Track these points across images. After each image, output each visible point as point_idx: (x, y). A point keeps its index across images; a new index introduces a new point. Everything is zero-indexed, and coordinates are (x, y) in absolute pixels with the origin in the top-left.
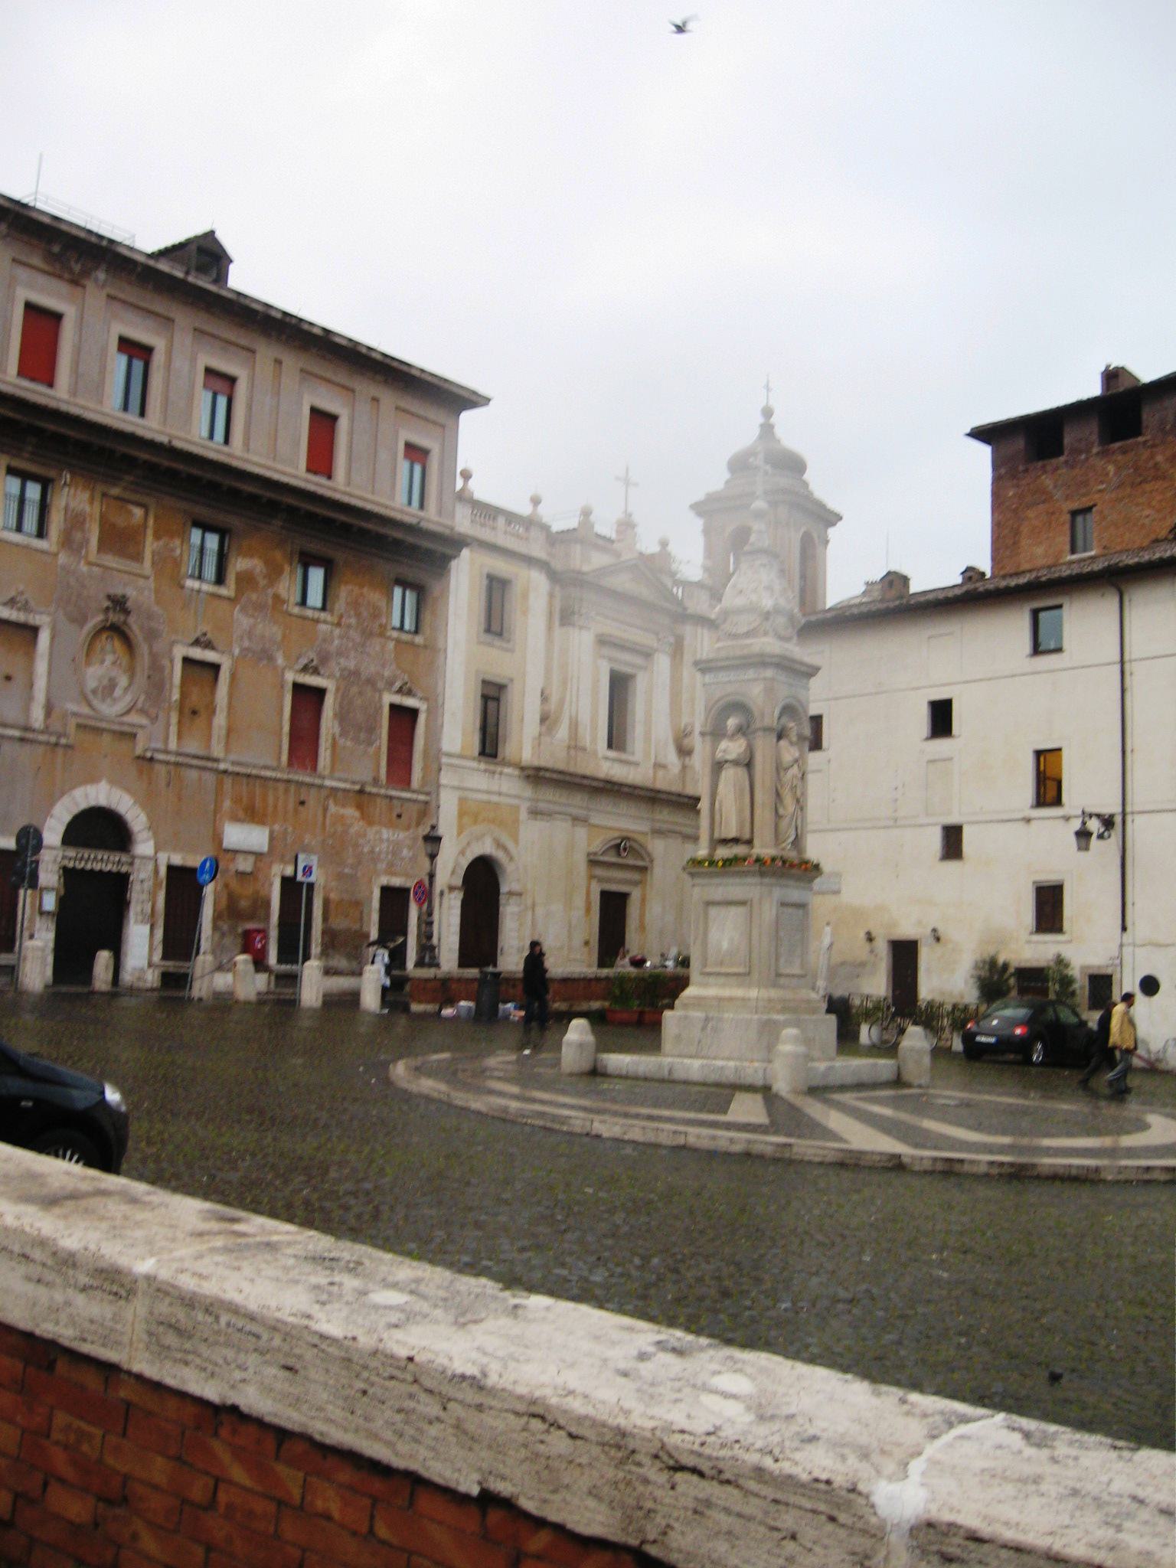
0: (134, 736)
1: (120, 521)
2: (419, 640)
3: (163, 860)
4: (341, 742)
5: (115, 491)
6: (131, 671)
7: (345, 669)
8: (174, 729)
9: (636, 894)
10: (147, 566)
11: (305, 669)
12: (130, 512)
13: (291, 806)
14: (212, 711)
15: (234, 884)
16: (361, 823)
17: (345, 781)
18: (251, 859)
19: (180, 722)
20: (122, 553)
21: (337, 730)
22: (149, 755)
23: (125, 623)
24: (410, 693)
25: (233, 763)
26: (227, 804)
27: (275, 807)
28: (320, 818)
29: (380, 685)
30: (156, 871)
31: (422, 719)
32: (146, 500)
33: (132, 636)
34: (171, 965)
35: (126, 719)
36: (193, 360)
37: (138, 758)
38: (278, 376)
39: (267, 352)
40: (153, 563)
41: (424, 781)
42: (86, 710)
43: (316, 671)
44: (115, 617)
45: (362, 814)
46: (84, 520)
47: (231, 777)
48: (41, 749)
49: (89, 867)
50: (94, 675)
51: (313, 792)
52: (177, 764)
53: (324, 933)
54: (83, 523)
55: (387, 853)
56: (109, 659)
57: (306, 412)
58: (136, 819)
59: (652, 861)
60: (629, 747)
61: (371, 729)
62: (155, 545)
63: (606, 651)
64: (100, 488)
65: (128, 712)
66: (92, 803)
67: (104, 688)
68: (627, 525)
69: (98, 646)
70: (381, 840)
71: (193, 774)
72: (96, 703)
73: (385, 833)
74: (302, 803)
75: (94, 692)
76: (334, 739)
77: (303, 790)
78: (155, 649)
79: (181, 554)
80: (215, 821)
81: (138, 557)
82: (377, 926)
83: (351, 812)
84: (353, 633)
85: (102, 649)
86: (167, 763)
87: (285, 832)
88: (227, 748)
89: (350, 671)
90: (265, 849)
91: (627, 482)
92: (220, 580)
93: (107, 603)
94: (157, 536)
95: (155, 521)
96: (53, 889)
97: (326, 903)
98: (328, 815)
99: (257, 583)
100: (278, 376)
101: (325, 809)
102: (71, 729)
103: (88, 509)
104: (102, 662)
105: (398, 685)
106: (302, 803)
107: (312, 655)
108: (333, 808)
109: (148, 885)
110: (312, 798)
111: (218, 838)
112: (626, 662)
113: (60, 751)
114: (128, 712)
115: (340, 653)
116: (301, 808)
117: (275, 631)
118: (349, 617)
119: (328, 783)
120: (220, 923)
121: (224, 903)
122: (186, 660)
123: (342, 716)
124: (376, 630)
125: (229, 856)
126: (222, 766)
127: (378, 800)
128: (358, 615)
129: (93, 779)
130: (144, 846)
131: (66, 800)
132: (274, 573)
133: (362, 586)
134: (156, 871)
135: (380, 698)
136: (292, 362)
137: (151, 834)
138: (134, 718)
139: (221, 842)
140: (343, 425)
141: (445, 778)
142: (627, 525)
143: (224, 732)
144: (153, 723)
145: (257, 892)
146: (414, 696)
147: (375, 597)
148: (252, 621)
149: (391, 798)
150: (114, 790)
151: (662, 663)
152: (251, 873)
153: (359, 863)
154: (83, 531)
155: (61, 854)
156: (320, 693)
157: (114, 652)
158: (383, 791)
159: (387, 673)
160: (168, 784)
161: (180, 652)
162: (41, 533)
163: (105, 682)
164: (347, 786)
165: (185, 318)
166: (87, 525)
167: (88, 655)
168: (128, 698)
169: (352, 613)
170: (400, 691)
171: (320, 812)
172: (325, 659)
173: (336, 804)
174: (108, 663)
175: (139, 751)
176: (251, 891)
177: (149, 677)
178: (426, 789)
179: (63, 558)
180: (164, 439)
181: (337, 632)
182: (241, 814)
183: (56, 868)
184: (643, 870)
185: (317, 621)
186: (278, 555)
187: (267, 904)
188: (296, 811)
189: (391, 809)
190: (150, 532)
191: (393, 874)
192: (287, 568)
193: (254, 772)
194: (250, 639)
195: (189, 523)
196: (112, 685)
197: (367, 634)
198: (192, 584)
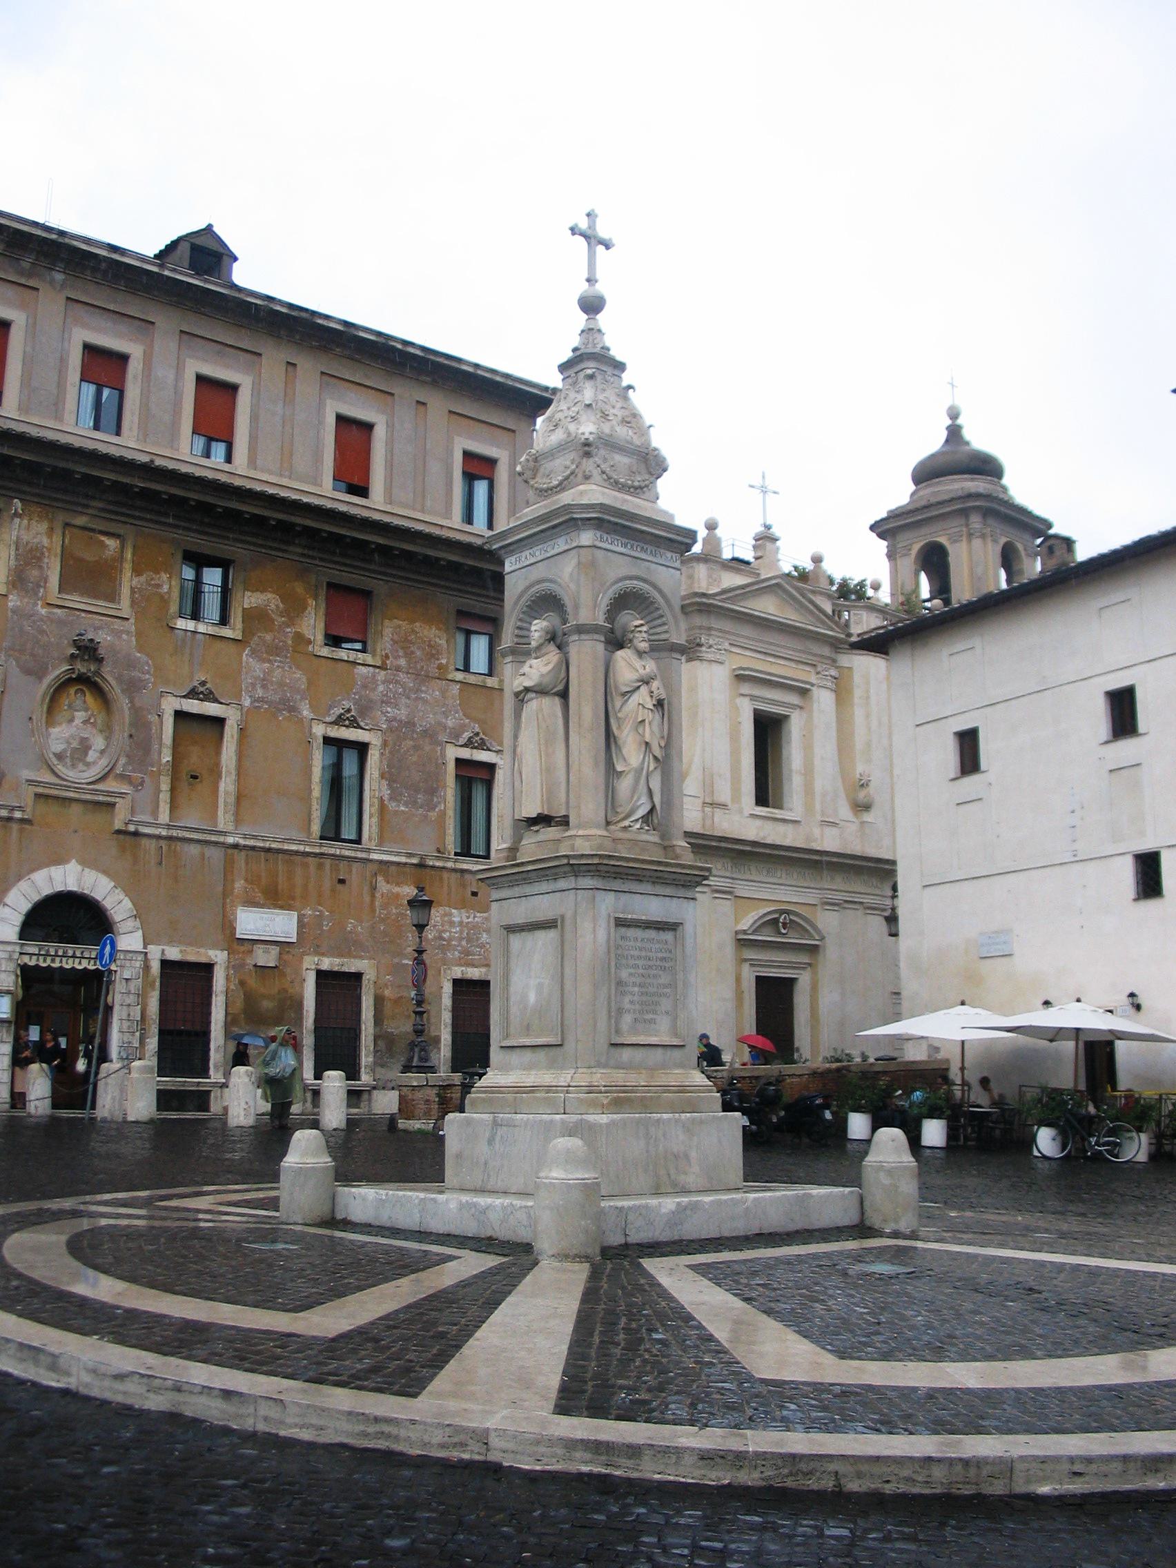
0: (112, 805)
1: (89, 556)
2: (491, 682)
3: (155, 952)
4: (392, 806)
5: (81, 521)
6: (107, 730)
7: (394, 719)
8: (165, 797)
9: (804, 980)
10: (125, 606)
11: (339, 722)
13: (327, 884)
14: (216, 772)
15: (252, 982)
17: (398, 854)
18: (275, 950)
19: (173, 790)
21: (386, 793)
22: (132, 828)
23: (97, 673)
24: (482, 746)
25: (245, 837)
26: (239, 885)
27: (305, 887)
28: (367, 899)
29: (443, 737)
30: (146, 967)
31: (500, 777)
32: (121, 530)
33: (106, 688)
34: (172, 1082)
36: (179, 369)
37: (119, 832)
38: (289, 382)
39: (274, 356)
40: (133, 603)
42: (49, 778)
43: (354, 724)
44: (81, 667)
46: (43, 554)
47: (243, 853)
49: (56, 965)
50: (60, 736)
51: (355, 866)
52: (170, 838)
53: (376, 1038)
54: (40, 559)
55: (461, 939)
56: (80, 716)
57: (331, 421)
58: (118, 905)
59: (823, 938)
60: (785, 805)
61: (433, 790)
63: (746, 688)
64: (62, 517)
65: (103, 779)
66: (59, 888)
67: (75, 750)
68: (765, 539)
69: (65, 701)
70: (452, 923)
71: (194, 850)
72: (60, 768)
73: (457, 915)
74: (342, 881)
75: (60, 756)
76: (381, 800)
78: (138, 704)
79: (169, 592)
81: (112, 597)
82: (449, 1029)
85: (70, 706)
86: (159, 837)
87: (321, 915)
88: (238, 821)
89: (401, 721)
90: (294, 940)
91: (764, 490)
92: (224, 621)
93: (73, 651)
94: (137, 571)
95: (134, 555)
96: (8, 992)
97: (379, 1001)
98: (378, 895)
99: (272, 621)
100: (289, 382)
101: (374, 888)
102: (29, 800)
104: (71, 720)
105: (466, 735)
106: (342, 881)
107: (347, 704)
108: (383, 886)
110: (355, 876)
111: (228, 926)
112: (775, 700)
113: (15, 827)
114: (103, 779)
116: (340, 887)
117: (299, 677)
119: (374, 856)
121: (239, 1004)
122: (180, 715)
123: (387, 775)
124: (434, 671)
125: (247, 947)
127: (445, 875)
128: (409, 655)
129: (59, 860)
130: (129, 940)
131: (23, 885)
132: (294, 609)
133: (412, 621)
134: (146, 967)
135: (443, 755)
136: (309, 366)
137: (138, 923)
138: (111, 785)
140: (380, 433)
142: (765, 539)
143: (232, 799)
145: (285, 991)
146: (490, 750)
147: (433, 634)
148: (267, 665)
149: (463, 871)
150: (87, 870)
151: (824, 699)
152: (276, 967)
154: (41, 567)
155: (18, 949)
156: (362, 749)
157: (86, 710)
158: (450, 865)
159: (450, 723)
161: (170, 705)
163: (75, 744)
164: (403, 860)
165: (167, 322)
166: (46, 560)
167: (50, 711)
168: (103, 762)
170: (469, 744)
171: (366, 889)
172: (365, 709)
174: (77, 722)
175: (118, 825)
176: (275, 991)
177: (131, 736)
179: (13, 601)
180: (144, 459)
181: (382, 675)
182: (259, 897)
183: (11, 966)
184: (813, 950)
185: (354, 663)
186: (299, 588)
187: (299, 1005)
188: (333, 891)
189: (463, 886)
190: (128, 566)
191: (468, 964)
192: (312, 602)
193: (274, 846)
194: (264, 687)
195: (179, 556)
196: (85, 746)
197: (423, 678)
198: (181, 624)
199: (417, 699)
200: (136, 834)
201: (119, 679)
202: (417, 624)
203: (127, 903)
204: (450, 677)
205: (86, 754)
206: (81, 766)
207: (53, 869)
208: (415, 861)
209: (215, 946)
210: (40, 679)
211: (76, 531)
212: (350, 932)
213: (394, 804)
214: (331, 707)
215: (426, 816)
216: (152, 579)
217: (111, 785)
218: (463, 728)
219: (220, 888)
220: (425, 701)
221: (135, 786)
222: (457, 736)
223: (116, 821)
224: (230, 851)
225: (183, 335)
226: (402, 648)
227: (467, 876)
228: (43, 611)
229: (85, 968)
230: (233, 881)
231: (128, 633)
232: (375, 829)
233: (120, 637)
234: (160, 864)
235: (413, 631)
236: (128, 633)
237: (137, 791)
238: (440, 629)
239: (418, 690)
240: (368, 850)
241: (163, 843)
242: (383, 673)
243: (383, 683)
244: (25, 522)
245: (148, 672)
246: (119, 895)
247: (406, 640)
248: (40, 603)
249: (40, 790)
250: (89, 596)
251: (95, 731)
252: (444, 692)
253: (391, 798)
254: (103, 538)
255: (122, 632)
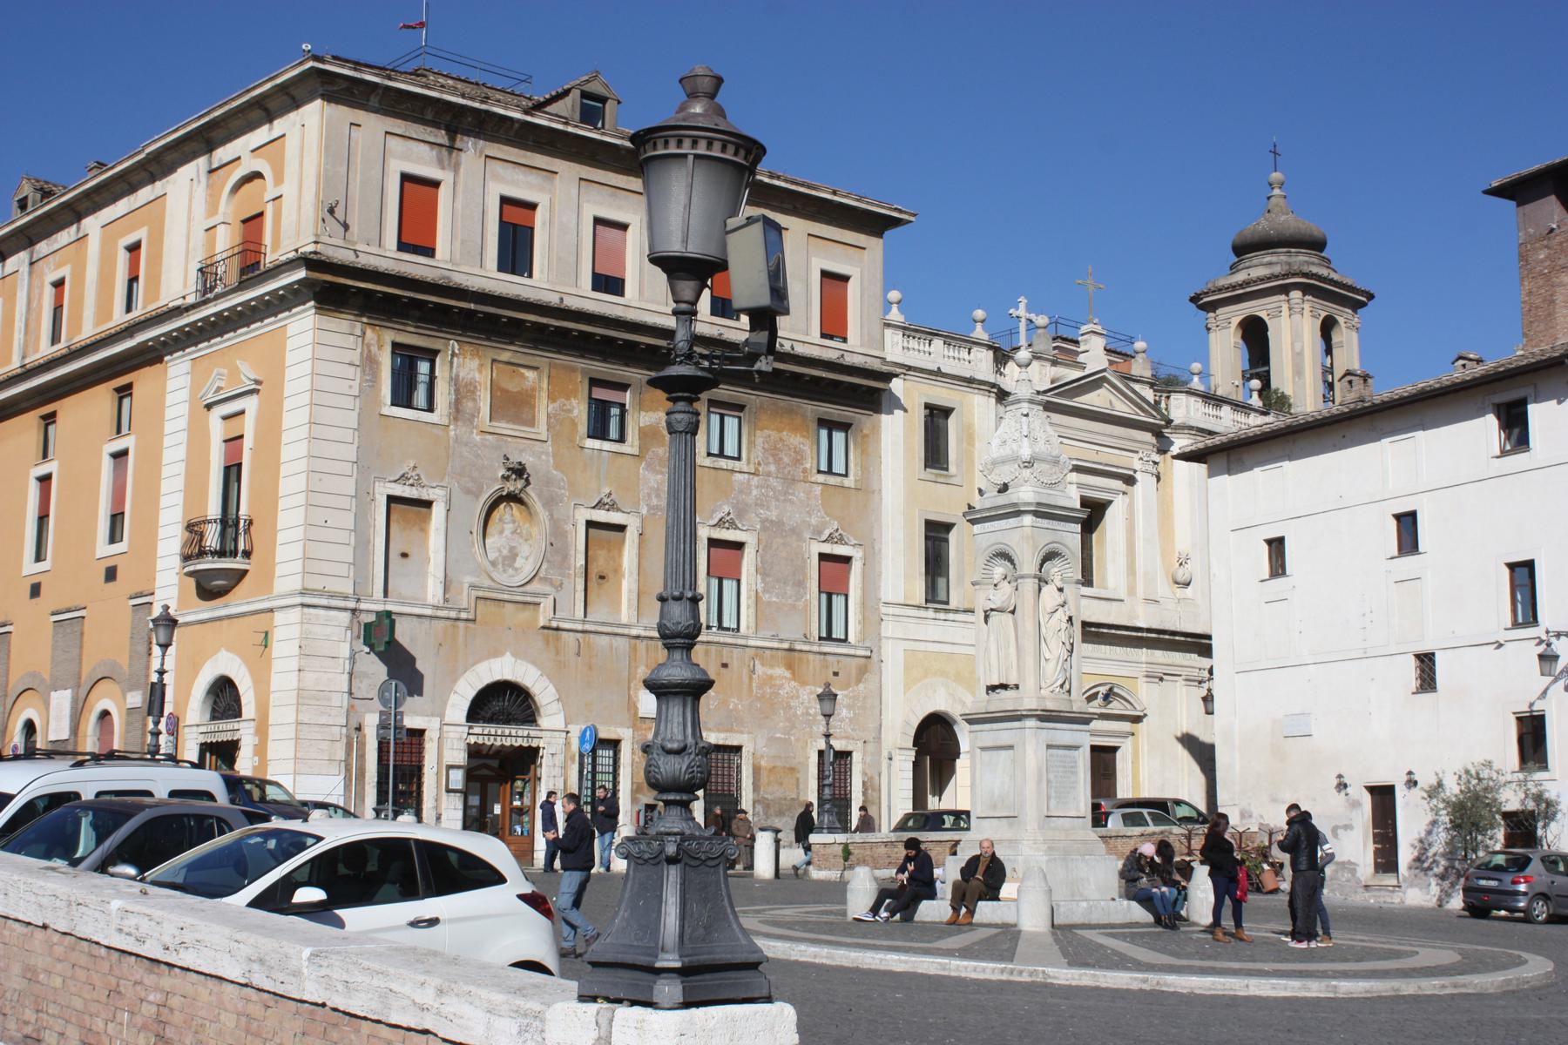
1: (512, 386)
4: (766, 598)
5: (505, 356)
7: (767, 520)
10: (542, 430)
12: (522, 375)
16: (793, 683)
20: (516, 419)
21: (760, 587)
22: (554, 624)
24: (841, 541)
28: (746, 679)
30: (567, 744)
31: (856, 568)
35: (528, 588)
37: (544, 628)
41: (864, 634)
43: (733, 525)
44: (514, 486)
45: (793, 674)
46: (475, 387)
47: (645, 642)
48: (442, 623)
51: (736, 651)
52: (583, 632)
54: (473, 392)
56: (509, 528)
58: (543, 691)
61: (801, 584)
62: (551, 406)
64: (492, 354)
67: (505, 558)
69: (496, 515)
71: (604, 640)
72: (495, 575)
74: (725, 665)
75: (494, 564)
77: (726, 650)
80: (629, 689)
81: (531, 422)
83: (780, 672)
84: (773, 482)
89: (772, 521)
94: (552, 398)
97: (757, 770)
101: (753, 671)
103: (477, 376)
104: (501, 532)
106: (725, 665)
108: (760, 669)
109: (559, 759)
115: (760, 504)
116: (724, 670)
118: (767, 464)
119: (751, 643)
120: (640, 796)
123: (762, 570)
126: (634, 632)
128: (778, 461)
129: (497, 653)
133: (780, 430)
134: (567, 744)
139: (636, 709)
141: (888, 629)
144: (558, 591)
146: (846, 544)
147: (795, 440)
148: (660, 476)
149: (825, 654)
153: (793, 727)
154: (474, 400)
157: (514, 522)
158: (815, 648)
159: (814, 521)
160: (578, 654)
161: (584, 515)
162: (430, 408)
163: (505, 552)
169: (771, 460)
170: (828, 540)
171: (745, 672)
172: (741, 512)
173: (763, 665)
174: (507, 532)
178: (868, 644)
183: (463, 746)
190: (544, 395)
199: (785, 501)
200: (557, 629)
201: (540, 496)
202: (785, 433)
203: (552, 689)
204: (813, 479)
205: (515, 560)
206: (511, 571)
207: (492, 660)
208: (786, 645)
209: (622, 725)
210: (477, 496)
211: (500, 365)
212: (732, 711)
213: (767, 596)
214: (713, 512)
215: (794, 606)
216: (564, 405)
217: (535, 587)
218: (824, 525)
219: (626, 674)
220: (792, 502)
221: (556, 588)
222: (820, 533)
223: (541, 618)
224: (633, 641)
225: (583, 183)
226: (773, 455)
227: (829, 658)
228: (478, 438)
229: (521, 746)
230: (636, 667)
231: (547, 454)
232: (752, 619)
233: (540, 458)
234: (578, 654)
235: (781, 439)
236: (547, 454)
237: (558, 591)
238: (804, 437)
239: (786, 493)
240: (746, 637)
241: (579, 635)
242: (756, 478)
243: (757, 487)
244: (461, 360)
245: (564, 488)
246: (545, 682)
247: (775, 448)
248: (475, 431)
249: (481, 594)
250: (514, 423)
251: (521, 541)
252: (808, 493)
253: (765, 591)
254: (523, 371)
255: (542, 453)
